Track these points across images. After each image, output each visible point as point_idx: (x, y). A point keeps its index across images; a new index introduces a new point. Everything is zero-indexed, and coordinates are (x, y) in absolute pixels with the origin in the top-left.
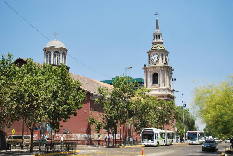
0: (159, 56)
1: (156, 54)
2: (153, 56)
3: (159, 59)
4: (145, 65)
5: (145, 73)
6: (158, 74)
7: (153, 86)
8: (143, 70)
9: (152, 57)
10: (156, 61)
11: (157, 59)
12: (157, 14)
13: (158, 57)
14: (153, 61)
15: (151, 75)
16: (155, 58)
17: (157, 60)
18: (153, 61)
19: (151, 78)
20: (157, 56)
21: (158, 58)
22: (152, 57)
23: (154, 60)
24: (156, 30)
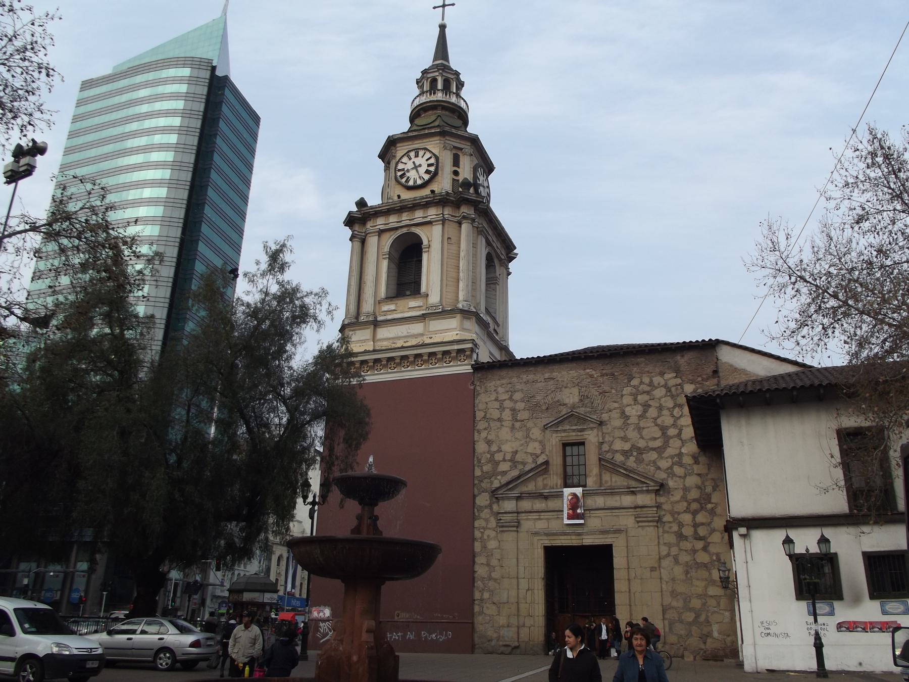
0: (437, 158)
1: (426, 149)
2: (405, 159)
3: (436, 174)
4: (361, 203)
5: (357, 244)
6: (425, 242)
7: (392, 307)
8: (348, 232)
9: (400, 166)
10: (419, 182)
11: (427, 172)
12: (444, 6)
13: (432, 161)
14: (404, 180)
15: (386, 249)
16: (416, 167)
17: (427, 177)
18: (404, 180)
19: (385, 264)
20: (428, 155)
21: (432, 169)
22: (400, 166)
23: (408, 180)
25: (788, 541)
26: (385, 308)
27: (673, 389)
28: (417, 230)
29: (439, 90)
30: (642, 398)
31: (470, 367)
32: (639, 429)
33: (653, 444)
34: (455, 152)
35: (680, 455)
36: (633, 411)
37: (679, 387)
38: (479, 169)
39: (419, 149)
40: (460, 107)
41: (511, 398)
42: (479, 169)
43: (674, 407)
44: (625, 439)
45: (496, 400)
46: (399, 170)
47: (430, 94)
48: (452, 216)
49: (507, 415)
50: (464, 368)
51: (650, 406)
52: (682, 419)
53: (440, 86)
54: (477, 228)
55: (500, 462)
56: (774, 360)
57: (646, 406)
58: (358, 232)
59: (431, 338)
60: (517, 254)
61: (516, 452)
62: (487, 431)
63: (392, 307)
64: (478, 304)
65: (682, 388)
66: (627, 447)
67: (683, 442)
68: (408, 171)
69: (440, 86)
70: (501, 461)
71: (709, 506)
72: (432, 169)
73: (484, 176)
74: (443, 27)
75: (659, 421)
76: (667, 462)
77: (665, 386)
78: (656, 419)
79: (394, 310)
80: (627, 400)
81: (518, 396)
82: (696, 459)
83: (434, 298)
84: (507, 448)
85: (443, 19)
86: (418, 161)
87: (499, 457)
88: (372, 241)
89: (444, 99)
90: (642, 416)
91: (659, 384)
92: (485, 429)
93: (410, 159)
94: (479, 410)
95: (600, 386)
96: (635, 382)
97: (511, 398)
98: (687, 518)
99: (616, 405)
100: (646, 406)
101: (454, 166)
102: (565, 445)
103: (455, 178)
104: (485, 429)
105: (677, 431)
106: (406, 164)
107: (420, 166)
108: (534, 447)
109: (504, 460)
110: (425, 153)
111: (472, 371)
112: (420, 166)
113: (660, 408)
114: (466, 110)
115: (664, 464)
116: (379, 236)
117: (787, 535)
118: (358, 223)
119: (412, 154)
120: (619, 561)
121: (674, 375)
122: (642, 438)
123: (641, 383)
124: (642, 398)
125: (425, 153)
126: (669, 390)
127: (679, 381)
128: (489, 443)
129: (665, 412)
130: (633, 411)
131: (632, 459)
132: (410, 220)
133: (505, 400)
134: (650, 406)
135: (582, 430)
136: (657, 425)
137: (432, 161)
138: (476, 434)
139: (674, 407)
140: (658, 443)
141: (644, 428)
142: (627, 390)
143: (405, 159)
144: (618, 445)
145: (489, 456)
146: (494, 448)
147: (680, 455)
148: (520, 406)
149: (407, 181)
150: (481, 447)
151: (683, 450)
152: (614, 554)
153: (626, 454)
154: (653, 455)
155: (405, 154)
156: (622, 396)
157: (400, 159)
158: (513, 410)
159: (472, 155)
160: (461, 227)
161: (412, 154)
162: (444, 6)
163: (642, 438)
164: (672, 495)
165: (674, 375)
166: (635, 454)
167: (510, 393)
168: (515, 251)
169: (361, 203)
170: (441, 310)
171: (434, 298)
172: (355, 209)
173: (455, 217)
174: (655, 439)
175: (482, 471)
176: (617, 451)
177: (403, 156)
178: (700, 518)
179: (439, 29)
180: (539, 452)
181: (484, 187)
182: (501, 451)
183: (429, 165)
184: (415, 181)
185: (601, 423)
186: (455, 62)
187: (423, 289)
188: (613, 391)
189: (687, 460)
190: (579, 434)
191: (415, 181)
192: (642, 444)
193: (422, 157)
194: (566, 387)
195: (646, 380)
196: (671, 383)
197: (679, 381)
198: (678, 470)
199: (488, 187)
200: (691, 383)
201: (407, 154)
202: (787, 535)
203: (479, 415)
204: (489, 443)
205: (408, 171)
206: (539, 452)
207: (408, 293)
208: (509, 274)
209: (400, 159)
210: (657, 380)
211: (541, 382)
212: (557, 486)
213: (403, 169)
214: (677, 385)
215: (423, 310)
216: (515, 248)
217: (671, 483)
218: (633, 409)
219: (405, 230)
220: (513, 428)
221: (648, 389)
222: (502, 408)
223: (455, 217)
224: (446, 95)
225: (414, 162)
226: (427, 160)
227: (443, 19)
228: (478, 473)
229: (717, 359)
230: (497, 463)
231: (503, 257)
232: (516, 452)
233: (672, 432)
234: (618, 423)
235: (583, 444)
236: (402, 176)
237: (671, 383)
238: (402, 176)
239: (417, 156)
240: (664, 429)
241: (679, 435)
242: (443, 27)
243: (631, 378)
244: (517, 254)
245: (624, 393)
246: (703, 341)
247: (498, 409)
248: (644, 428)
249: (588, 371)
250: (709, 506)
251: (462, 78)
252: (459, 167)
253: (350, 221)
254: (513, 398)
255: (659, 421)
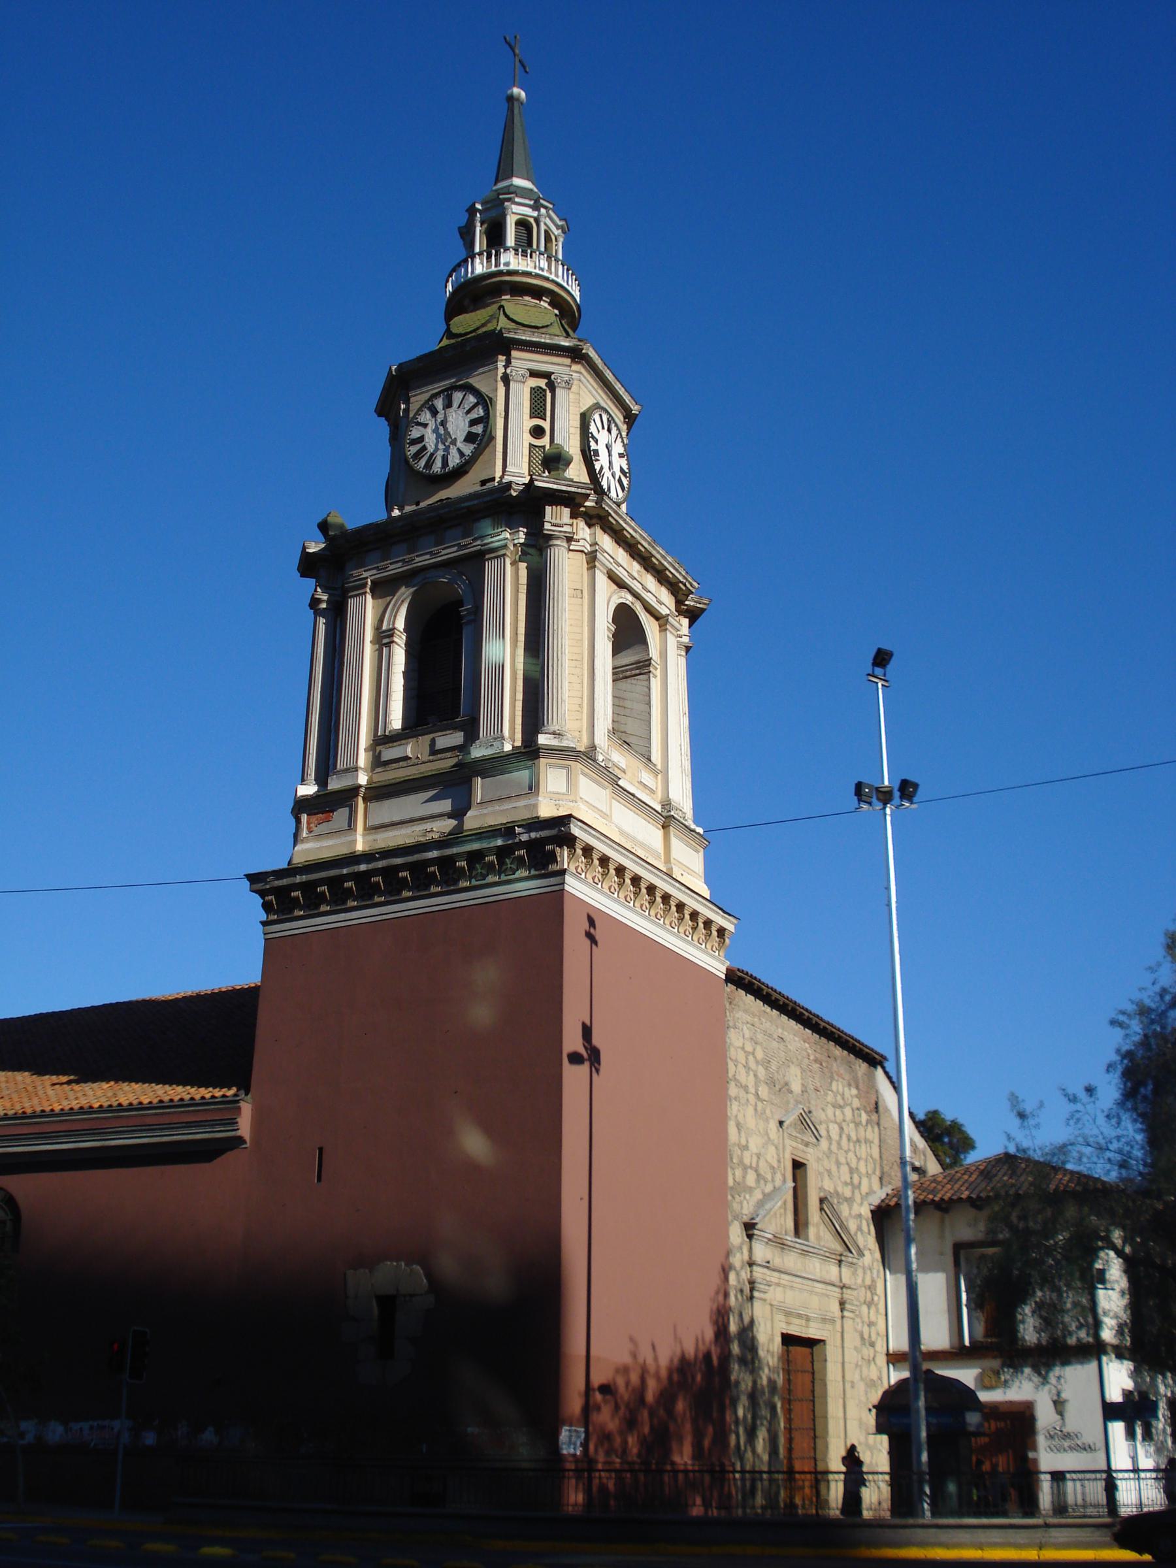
17: (468, 449)
24: (501, 185)
38: (596, 417)
42: (596, 417)
46: (414, 442)
72: (478, 429)
73: (609, 431)
119: (439, 403)
125: (464, 396)
149: (429, 465)
155: (423, 406)
177: (420, 410)
183: (473, 423)
226: (468, 412)
231: (664, 611)
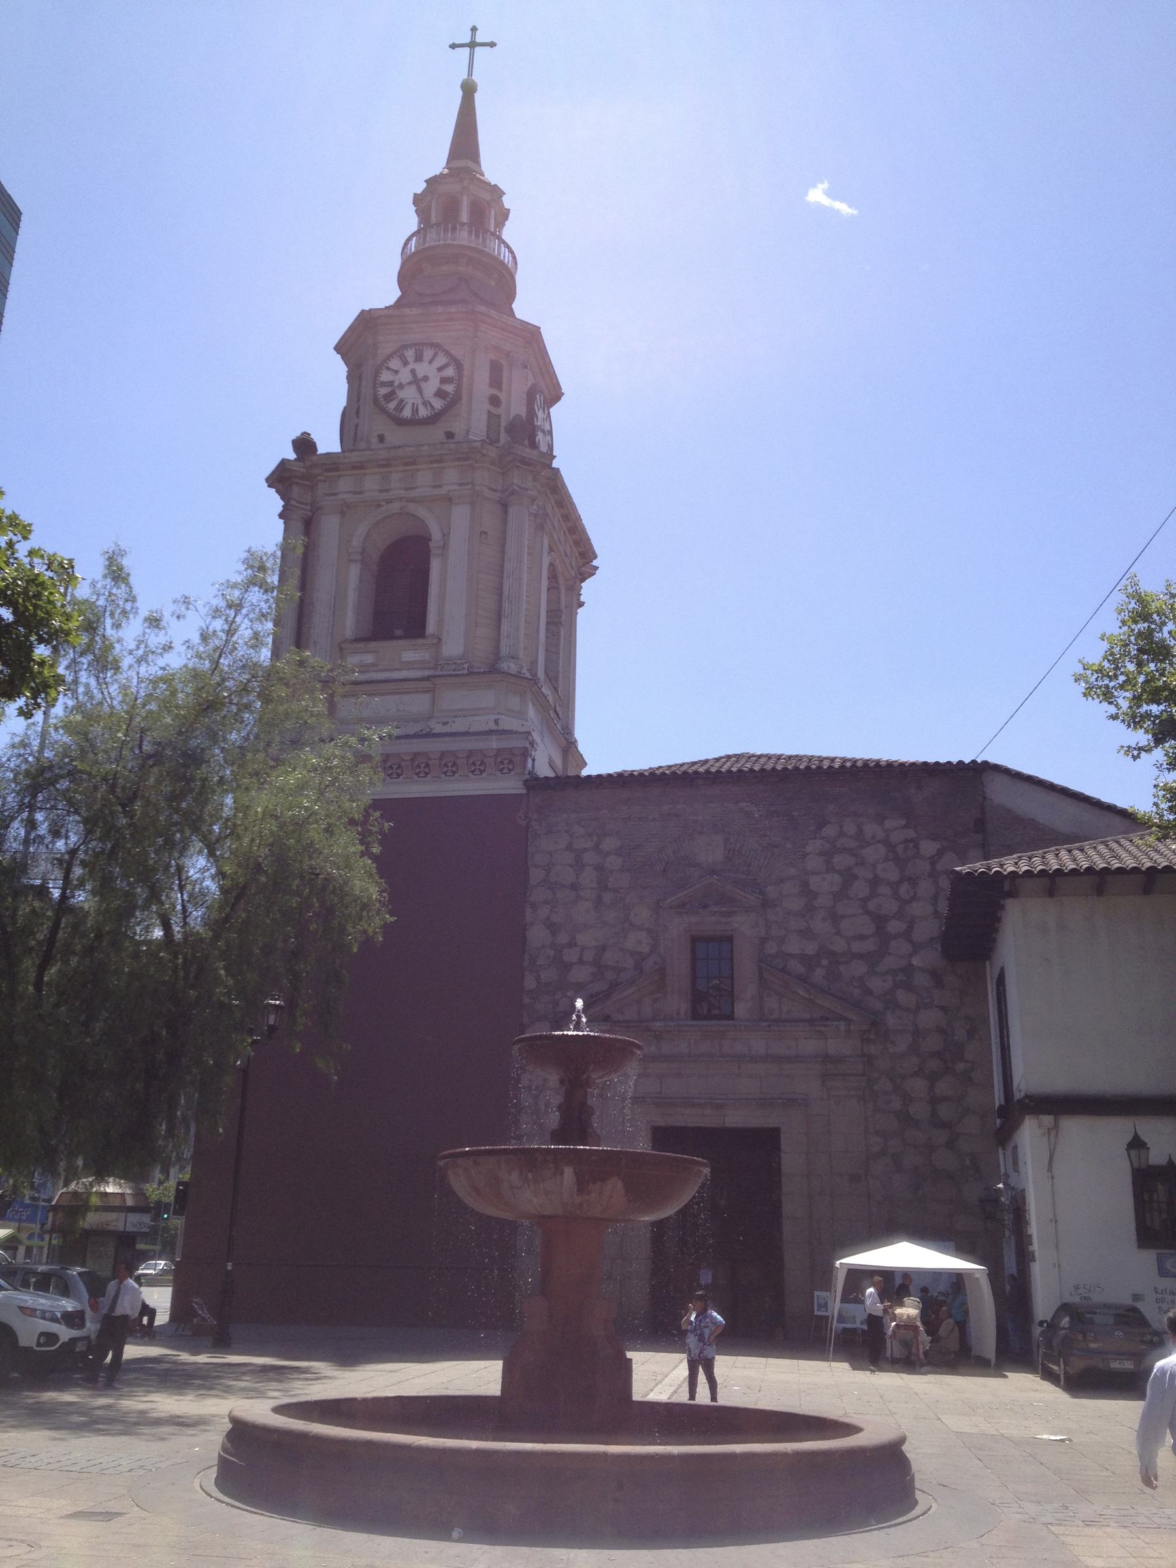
2: (395, 364)
4: (304, 445)
6: (436, 535)
7: (369, 659)
9: (385, 376)
10: (423, 412)
11: (440, 394)
12: (472, 45)
14: (392, 406)
15: (357, 542)
17: (438, 404)
18: (392, 406)
19: (354, 571)
20: (441, 360)
22: (385, 376)
23: (401, 406)
25: (1136, 1144)
26: (353, 660)
27: (900, 849)
28: (421, 512)
29: (462, 224)
30: (840, 861)
31: (520, 784)
32: (835, 918)
33: (857, 947)
34: (493, 358)
35: (909, 970)
36: (824, 884)
37: (911, 845)
38: (538, 396)
39: (424, 344)
40: (502, 263)
41: (596, 848)
42: (538, 396)
43: (901, 881)
44: (806, 934)
45: (569, 848)
46: (384, 384)
47: (446, 230)
48: (490, 489)
49: (588, 877)
50: (509, 785)
51: (855, 877)
52: (914, 905)
53: (464, 217)
54: (536, 516)
55: (571, 964)
56: (1089, 807)
57: (849, 878)
58: (298, 502)
59: (445, 724)
60: (597, 568)
61: (604, 948)
62: (549, 906)
63: (369, 659)
64: (534, 662)
65: (916, 846)
66: (811, 948)
67: (916, 948)
68: (401, 386)
69: (464, 217)
70: (575, 964)
71: (960, 1067)
73: (544, 411)
74: (469, 90)
75: (872, 905)
76: (884, 981)
77: (886, 842)
78: (865, 900)
79: (373, 665)
80: (814, 863)
81: (609, 844)
82: (936, 977)
83: (453, 647)
84: (586, 939)
85: (470, 73)
86: (422, 369)
87: (571, 956)
88: (330, 525)
89: (473, 245)
90: (840, 895)
91: (874, 837)
92: (546, 902)
93: (406, 363)
94: (535, 866)
95: (765, 835)
96: (830, 831)
97: (596, 848)
98: (918, 1086)
99: (792, 871)
100: (849, 878)
101: (491, 385)
102: (695, 940)
103: (495, 411)
104: (546, 902)
105: (904, 926)
106: (396, 372)
107: (426, 378)
108: (637, 941)
109: (581, 961)
110: (436, 355)
111: (525, 791)
112: (426, 378)
113: (875, 882)
114: (513, 271)
115: (878, 985)
116: (343, 514)
117: (1136, 1133)
118: (297, 483)
119: (410, 354)
120: (791, 1159)
121: (903, 822)
122: (838, 933)
123: (842, 834)
124: (840, 861)
125: (436, 355)
126: (890, 846)
127: (911, 834)
128: (553, 928)
129: (884, 889)
130: (824, 884)
131: (819, 973)
132: (406, 489)
133: (585, 850)
134: (855, 877)
135: (730, 914)
136: (867, 912)
137: (450, 372)
138: (529, 910)
139: (901, 881)
140: (868, 946)
141: (843, 917)
142: (813, 846)
143: (395, 364)
144: (794, 946)
145: (552, 953)
146: (563, 938)
147: (909, 970)
148: (614, 862)
150: (537, 935)
151: (915, 961)
152: (783, 1147)
153: (809, 961)
154: (859, 968)
156: (805, 855)
157: (385, 361)
158: (599, 868)
159: (526, 367)
160: (506, 512)
161: (410, 354)
162: (472, 45)
163: (838, 933)
164: (893, 1042)
165: (903, 822)
166: (825, 962)
167: (595, 838)
168: (595, 563)
169: (304, 445)
170: (466, 672)
171: (453, 647)
172: (292, 456)
173: (496, 491)
174: (862, 938)
175: (538, 979)
176: (791, 955)
178: (943, 1087)
179: (460, 93)
180: (645, 949)
181: (543, 431)
182: (576, 945)
183: (444, 381)
184: (415, 410)
185: (766, 904)
186: (493, 168)
187: (431, 627)
188: (789, 846)
189: (921, 980)
190: (724, 920)
191: (415, 410)
192: (839, 945)
193: (430, 362)
194: (700, 833)
195: (850, 829)
196: (896, 837)
197: (911, 834)
198: (902, 996)
199: (550, 433)
200: (933, 839)
201: (399, 353)
202: (1136, 1133)
203: (536, 875)
204: (553, 928)
205: (401, 386)
206: (645, 949)
207: (399, 632)
208: (581, 604)
209: (385, 361)
210: (870, 829)
211: (654, 820)
212: (678, 1014)
213: (391, 383)
214: (907, 841)
215: (429, 669)
216: (595, 557)
217: (891, 1020)
218: (824, 879)
219: (395, 507)
220: (598, 902)
221: (853, 844)
222: (579, 865)
223: (496, 491)
224: (477, 236)
225: (413, 371)
226: (440, 369)
227: (470, 73)
228: (530, 983)
229: (984, 798)
230: (568, 967)
232: (604, 948)
233: (895, 926)
234: (796, 904)
235: (730, 939)
236: (389, 397)
237: (896, 837)
238: (389, 397)
239: (419, 358)
240: (880, 921)
241: (907, 934)
242: (469, 90)
243: (822, 823)
244: (597, 568)
245: (809, 849)
246: (960, 762)
247: (571, 866)
248: (843, 917)
249: (743, 804)
250: (960, 1067)
251: (507, 202)
252: (500, 388)
253: (281, 479)
254: (601, 847)
255: (872, 905)
